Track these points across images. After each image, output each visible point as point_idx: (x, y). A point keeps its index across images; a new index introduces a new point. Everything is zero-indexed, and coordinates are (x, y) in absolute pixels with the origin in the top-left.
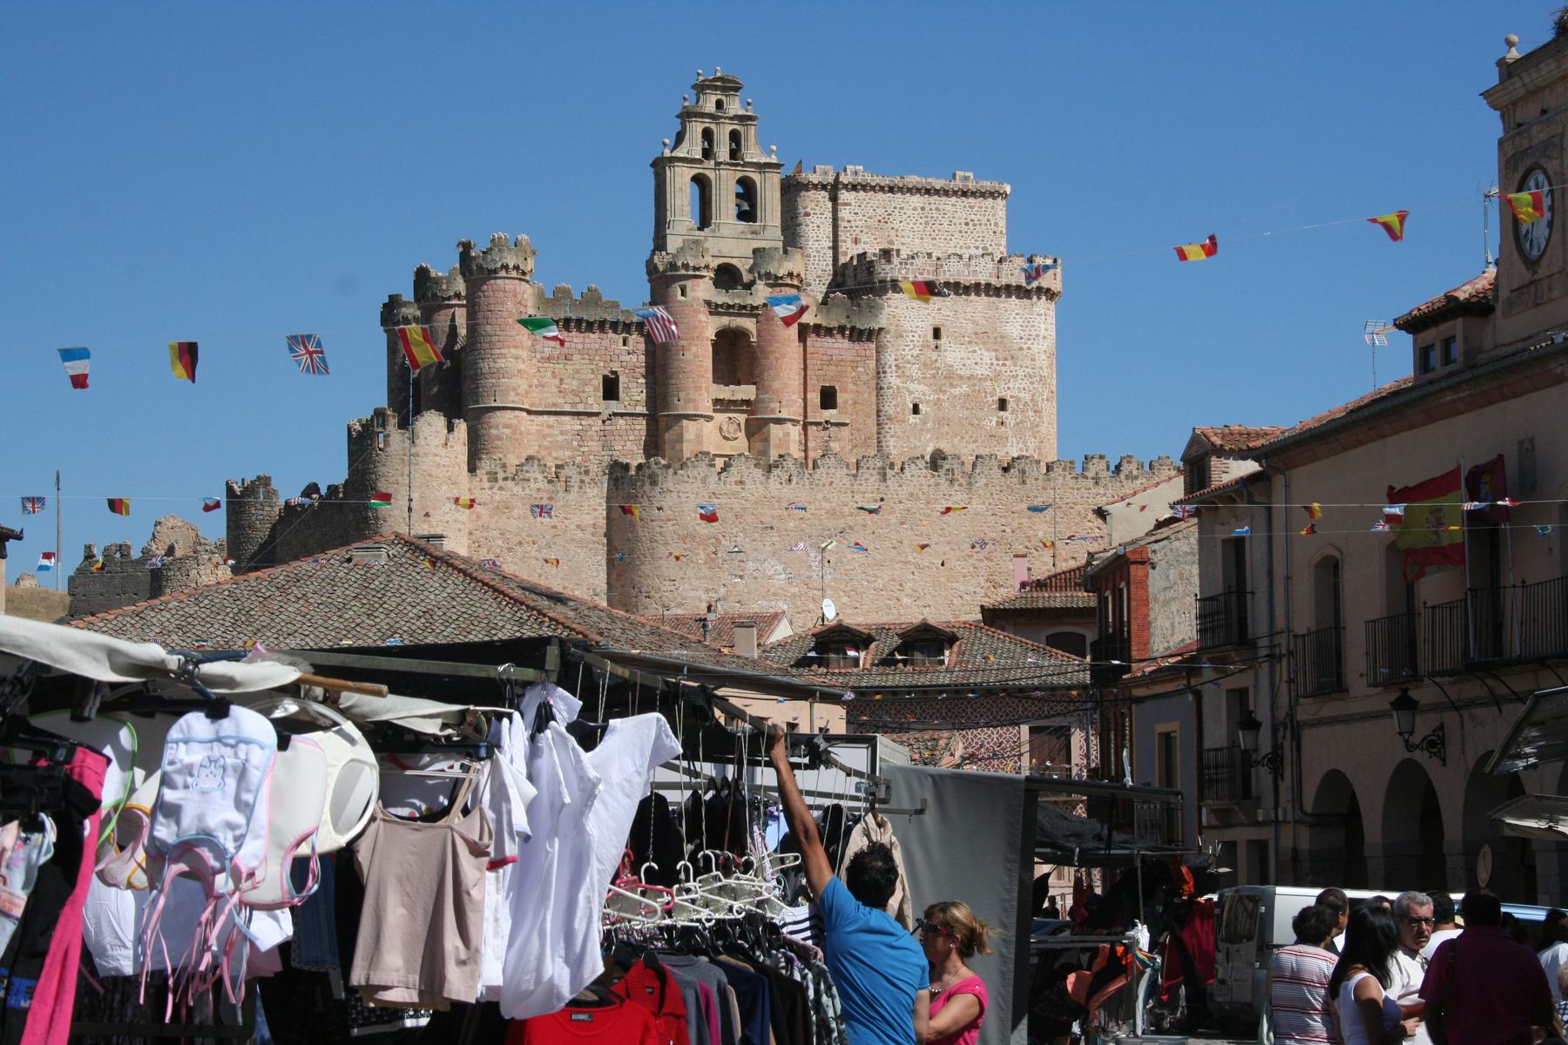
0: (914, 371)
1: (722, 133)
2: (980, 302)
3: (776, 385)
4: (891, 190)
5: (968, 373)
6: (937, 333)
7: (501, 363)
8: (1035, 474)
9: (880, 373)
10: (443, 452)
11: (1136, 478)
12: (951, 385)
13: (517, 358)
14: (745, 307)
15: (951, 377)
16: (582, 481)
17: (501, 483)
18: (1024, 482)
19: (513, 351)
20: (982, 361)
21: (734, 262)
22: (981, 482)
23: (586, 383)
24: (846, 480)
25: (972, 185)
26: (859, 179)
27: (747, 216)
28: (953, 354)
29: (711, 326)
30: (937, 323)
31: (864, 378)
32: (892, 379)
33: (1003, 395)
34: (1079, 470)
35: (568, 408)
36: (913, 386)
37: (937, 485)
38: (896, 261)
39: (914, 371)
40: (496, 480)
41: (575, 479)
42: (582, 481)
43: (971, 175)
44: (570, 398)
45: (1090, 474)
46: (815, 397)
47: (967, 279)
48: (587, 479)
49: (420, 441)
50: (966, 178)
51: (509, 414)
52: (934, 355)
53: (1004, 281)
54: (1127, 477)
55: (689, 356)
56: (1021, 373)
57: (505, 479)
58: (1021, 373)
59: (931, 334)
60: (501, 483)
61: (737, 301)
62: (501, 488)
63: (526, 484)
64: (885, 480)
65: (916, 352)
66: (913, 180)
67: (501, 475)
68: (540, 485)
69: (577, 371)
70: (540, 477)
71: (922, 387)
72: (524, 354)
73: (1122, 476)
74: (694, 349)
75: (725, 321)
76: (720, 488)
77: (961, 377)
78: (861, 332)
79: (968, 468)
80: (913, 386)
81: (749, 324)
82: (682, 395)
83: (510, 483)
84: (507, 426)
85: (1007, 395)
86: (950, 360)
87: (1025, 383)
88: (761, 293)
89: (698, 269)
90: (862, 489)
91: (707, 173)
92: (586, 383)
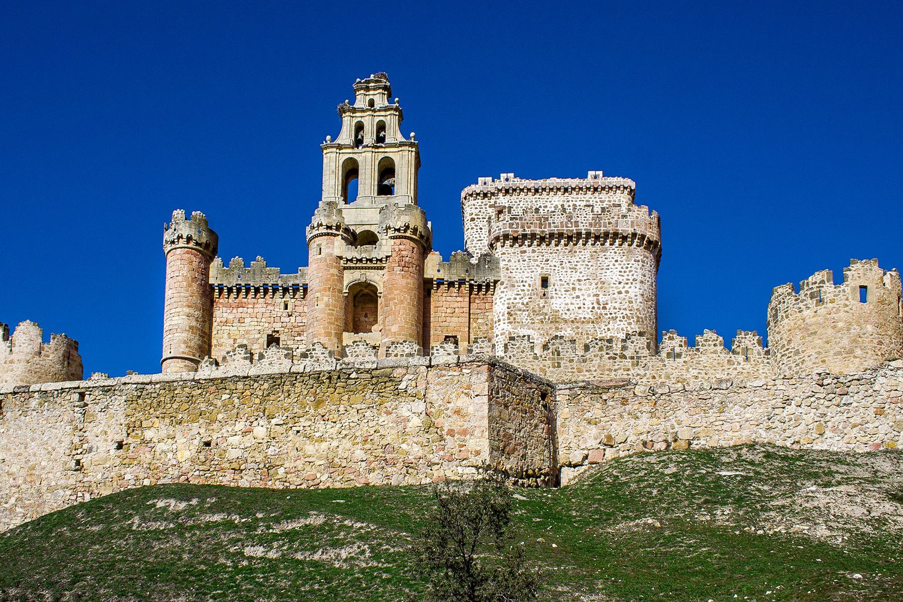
0: (523, 317)
5: (573, 316)
28: (559, 302)
78: (480, 287)
86: (554, 307)
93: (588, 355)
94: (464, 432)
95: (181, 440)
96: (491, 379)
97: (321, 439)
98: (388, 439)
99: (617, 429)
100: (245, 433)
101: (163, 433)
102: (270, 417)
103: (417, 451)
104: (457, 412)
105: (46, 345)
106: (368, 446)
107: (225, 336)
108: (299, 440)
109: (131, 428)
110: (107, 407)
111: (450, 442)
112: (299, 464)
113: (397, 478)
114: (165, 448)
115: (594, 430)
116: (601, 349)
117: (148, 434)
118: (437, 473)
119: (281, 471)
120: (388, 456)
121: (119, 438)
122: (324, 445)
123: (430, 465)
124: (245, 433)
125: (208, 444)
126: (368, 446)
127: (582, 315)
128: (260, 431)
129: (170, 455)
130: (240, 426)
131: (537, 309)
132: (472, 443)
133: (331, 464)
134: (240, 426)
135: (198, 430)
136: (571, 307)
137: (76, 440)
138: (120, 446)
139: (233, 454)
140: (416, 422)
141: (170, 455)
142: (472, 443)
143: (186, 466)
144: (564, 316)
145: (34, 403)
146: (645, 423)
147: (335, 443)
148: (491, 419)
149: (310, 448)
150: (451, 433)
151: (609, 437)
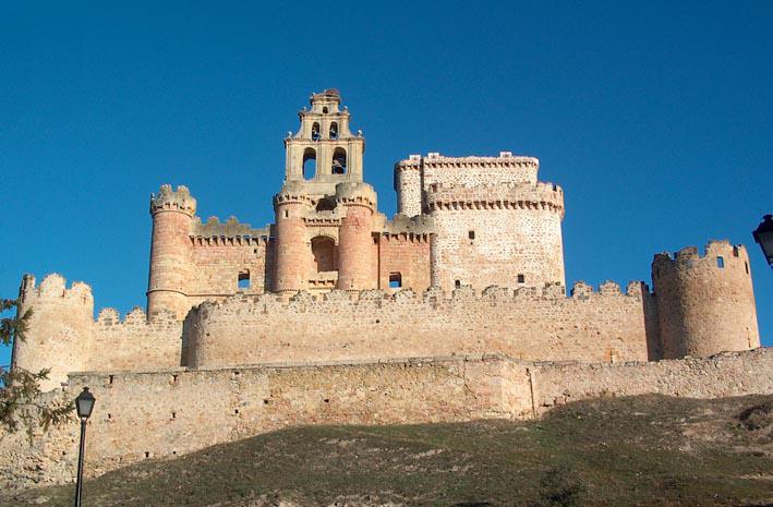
2: (504, 213)
3: (350, 269)
6: (472, 235)
7: (162, 263)
8: (504, 298)
9: (432, 262)
10: (60, 301)
11: (587, 298)
12: (483, 268)
13: (173, 260)
15: (482, 261)
18: (495, 305)
19: (171, 256)
23: (227, 277)
25: (511, 158)
27: (338, 170)
28: (483, 247)
29: (307, 235)
30: (471, 229)
31: (422, 267)
32: (440, 265)
33: (521, 272)
34: (539, 292)
35: (214, 293)
38: (439, 190)
40: (111, 324)
44: (215, 287)
46: (385, 280)
48: (174, 321)
49: (43, 294)
50: (506, 156)
51: (165, 294)
52: (470, 249)
55: (288, 252)
57: (117, 323)
58: (533, 257)
61: (323, 217)
62: (113, 329)
63: (130, 326)
64: (380, 307)
65: (457, 247)
67: (115, 320)
68: (141, 326)
69: (222, 270)
72: (181, 258)
73: (575, 296)
74: (291, 248)
76: (251, 317)
77: (490, 262)
79: (449, 296)
80: (454, 270)
81: (333, 232)
82: (283, 278)
83: (120, 325)
84: (163, 302)
85: (524, 272)
87: (537, 264)
88: (341, 211)
92: (227, 277)
93: (517, 298)
94: (490, 394)
97: (401, 398)
98: (443, 398)
99: (570, 387)
102: (367, 386)
103: (461, 404)
105: (68, 291)
107: (203, 273)
113: (450, 418)
116: (527, 294)
117: (286, 396)
118: (474, 415)
119: (376, 415)
121: (265, 397)
123: (469, 411)
125: (327, 401)
127: (502, 257)
128: (361, 394)
134: (349, 390)
136: (494, 252)
138: (266, 402)
140: (459, 389)
151: (567, 391)
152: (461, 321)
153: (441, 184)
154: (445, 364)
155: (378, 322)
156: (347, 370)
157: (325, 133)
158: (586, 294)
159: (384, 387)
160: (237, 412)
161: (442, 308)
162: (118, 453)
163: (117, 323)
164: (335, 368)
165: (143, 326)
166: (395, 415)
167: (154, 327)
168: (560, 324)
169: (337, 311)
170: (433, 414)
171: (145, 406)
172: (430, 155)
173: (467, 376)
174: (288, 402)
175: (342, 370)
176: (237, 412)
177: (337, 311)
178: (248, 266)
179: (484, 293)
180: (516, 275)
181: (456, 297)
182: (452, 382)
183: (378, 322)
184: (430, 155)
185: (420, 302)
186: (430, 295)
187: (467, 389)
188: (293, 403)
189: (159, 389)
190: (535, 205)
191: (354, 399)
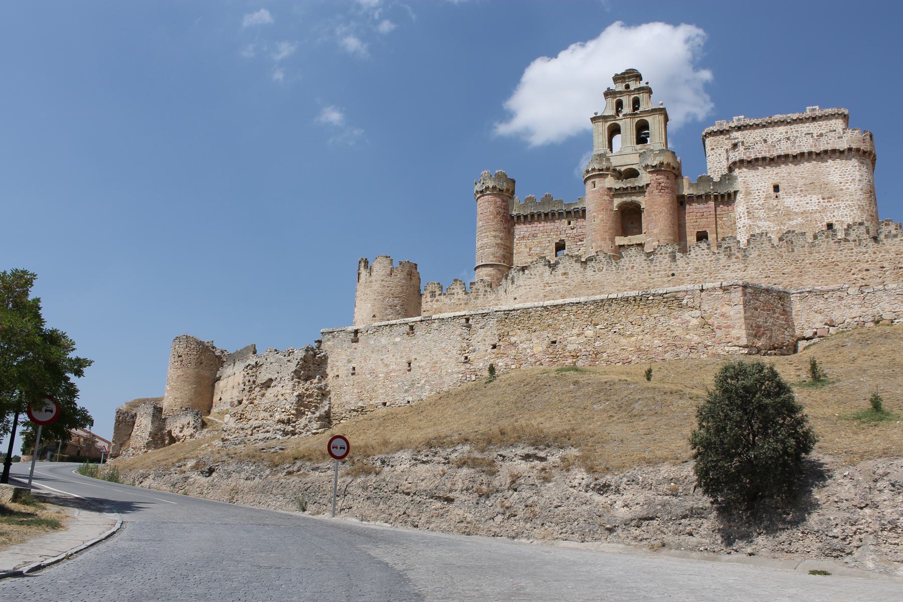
0: (761, 214)
1: (627, 101)
2: (807, 167)
4: (764, 126)
5: (802, 210)
6: (776, 188)
8: (801, 242)
11: (895, 236)
12: (790, 219)
14: (635, 188)
15: (788, 214)
16: (486, 291)
17: (437, 297)
18: (793, 251)
20: (813, 202)
21: (634, 167)
22: (754, 254)
24: (644, 264)
25: (818, 113)
26: (742, 123)
27: (641, 139)
28: (789, 201)
30: (776, 182)
33: (830, 221)
34: (840, 235)
36: (760, 223)
37: (718, 259)
39: (761, 214)
41: (482, 290)
42: (486, 291)
43: (817, 107)
45: (850, 238)
47: (796, 151)
52: (775, 202)
53: (822, 148)
54: (886, 236)
56: (842, 205)
57: (440, 295)
58: (842, 205)
59: (771, 190)
60: (437, 297)
62: (437, 301)
64: (675, 261)
66: (777, 117)
67: (438, 293)
68: (460, 296)
69: (540, 243)
70: (460, 291)
71: (768, 223)
75: (625, 199)
77: (796, 214)
78: (723, 196)
80: (760, 223)
83: (442, 297)
89: (602, 170)
90: (657, 268)
91: (617, 122)
94: (728, 327)
95: (535, 341)
96: (745, 294)
97: (632, 335)
98: (677, 333)
99: (837, 316)
100: (578, 335)
101: (523, 338)
103: (696, 339)
104: (722, 315)
106: (663, 338)
108: (616, 337)
109: (501, 337)
110: (485, 325)
111: (719, 333)
112: (618, 352)
114: (525, 346)
115: (820, 317)
117: (513, 339)
120: (677, 343)
121: (493, 343)
122: (633, 339)
124: (578, 335)
125: (554, 342)
126: (663, 338)
127: (810, 208)
128: (589, 332)
129: (529, 350)
130: (576, 331)
131: (771, 206)
132: (734, 333)
133: (639, 350)
134: (576, 331)
135: (549, 335)
137: (465, 345)
138: (494, 347)
139: (570, 347)
141: (529, 350)
142: (734, 333)
143: (539, 357)
144: (797, 211)
145: (435, 325)
146: (856, 311)
147: (640, 337)
148: (746, 318)
149: (623, 341)
150: (719, 328)
151: (832, 321)
152: (757, 269)
153: (743, 142)
154: (679, 295)
155: (673, 275)
156: (575, 308)
157: (627, 109)
158: (894, 232)
159: (613, 324)
160: (466, 358)
161: (737, 258)
162: (360, 404)
163: (440, 295)
164: (560, 307)
165: (462, 295)
166: (624, 355)
167: (472, 296)
168: (866, 266)
169: (633, 267)
170: (668, 351)
171: (384, 357)
172: (735, 118)
173: (705, 307)
174: (514, 344)
175: (569, 308)
176: (466, 358)
177: (633, 267)
178: (563, 237)
179: (781, 239)
180: (825, 223)
181: (751, 246)
182: (687, 315)
183: (673, 275)
184: (735, 118)
185: (714, 254)
186: (727, 246)
187: (704, 324)
188: (521, 346)
189: (398, 339)
190: (842, 152)
191: (582, 339)
